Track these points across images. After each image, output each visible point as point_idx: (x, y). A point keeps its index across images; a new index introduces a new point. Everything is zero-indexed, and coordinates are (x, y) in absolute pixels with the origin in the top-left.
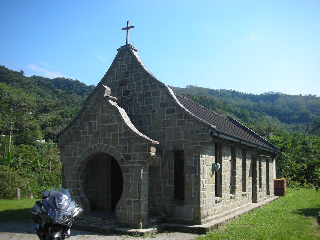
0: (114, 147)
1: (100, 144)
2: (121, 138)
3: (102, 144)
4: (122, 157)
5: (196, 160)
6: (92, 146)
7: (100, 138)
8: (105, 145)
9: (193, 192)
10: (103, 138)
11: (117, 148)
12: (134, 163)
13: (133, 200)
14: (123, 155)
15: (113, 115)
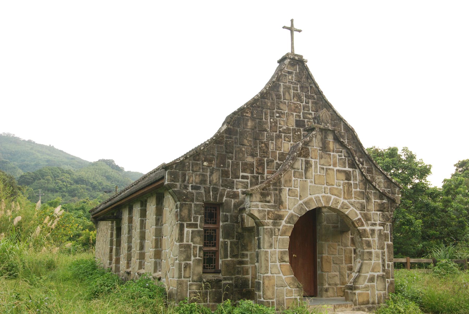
0: (346, 201)
1: (326, 195)
2: (356, 190)
3: (329, 195)
4: (360, 216)
6: (313, 197)
7: (325, 186)
8: (333, 197)
10: (329, 187)
14: (361, 214)
15: (343, 157)
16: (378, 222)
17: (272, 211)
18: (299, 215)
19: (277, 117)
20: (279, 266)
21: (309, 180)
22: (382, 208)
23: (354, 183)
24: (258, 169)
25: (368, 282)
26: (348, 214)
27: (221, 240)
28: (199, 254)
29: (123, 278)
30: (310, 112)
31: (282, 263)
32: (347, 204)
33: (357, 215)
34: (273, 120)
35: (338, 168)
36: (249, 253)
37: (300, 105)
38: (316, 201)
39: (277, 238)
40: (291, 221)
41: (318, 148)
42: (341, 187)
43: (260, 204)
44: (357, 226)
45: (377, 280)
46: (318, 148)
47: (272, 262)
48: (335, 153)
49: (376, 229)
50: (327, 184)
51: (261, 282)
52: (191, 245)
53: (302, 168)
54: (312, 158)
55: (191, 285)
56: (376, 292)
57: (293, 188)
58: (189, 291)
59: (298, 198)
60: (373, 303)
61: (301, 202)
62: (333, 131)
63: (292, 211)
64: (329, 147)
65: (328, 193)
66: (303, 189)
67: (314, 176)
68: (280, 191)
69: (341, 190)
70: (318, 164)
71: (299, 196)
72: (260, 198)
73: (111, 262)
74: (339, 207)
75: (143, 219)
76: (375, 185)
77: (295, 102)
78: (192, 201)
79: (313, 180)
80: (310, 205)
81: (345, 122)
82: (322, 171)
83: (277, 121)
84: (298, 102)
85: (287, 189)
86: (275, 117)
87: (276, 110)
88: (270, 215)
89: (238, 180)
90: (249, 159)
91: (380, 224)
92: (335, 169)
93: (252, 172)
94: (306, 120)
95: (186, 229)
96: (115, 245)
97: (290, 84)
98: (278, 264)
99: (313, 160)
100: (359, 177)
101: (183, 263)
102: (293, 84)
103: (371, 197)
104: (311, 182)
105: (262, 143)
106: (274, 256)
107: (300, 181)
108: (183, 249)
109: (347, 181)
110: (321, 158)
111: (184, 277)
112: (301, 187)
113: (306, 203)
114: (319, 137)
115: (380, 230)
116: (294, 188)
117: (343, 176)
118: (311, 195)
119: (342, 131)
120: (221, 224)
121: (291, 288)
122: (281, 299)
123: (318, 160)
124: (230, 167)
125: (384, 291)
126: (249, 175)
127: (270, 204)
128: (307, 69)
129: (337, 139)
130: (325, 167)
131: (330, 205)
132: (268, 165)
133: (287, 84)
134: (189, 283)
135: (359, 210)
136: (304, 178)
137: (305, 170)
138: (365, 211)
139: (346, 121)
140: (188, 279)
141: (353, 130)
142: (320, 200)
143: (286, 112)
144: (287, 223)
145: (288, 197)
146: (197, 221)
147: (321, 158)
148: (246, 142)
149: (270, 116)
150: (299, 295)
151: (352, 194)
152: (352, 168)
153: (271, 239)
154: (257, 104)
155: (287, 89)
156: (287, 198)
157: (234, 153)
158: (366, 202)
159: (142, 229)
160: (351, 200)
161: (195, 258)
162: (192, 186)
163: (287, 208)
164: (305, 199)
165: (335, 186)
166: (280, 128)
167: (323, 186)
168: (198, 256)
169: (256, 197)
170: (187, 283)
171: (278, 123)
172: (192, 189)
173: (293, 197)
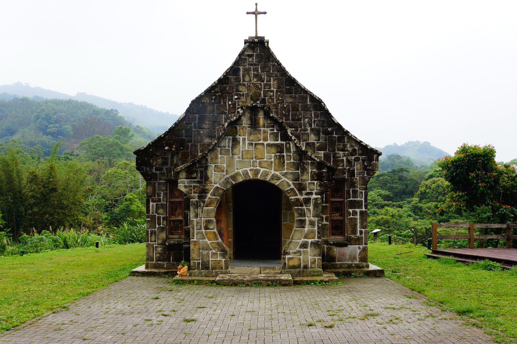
0: (278, 173)
2: (289, 161)
3: (258, 168)
4: (292, 186)
5: (362, 193)
7: (254, 159)
8: (262, 170)
9: (359, 229)
10: (258, 161)
11: (285, 175)
12: (311, 194)
13: (310, 241)
14: (293, 184)
15: (275, 131)
16: (314, 192)
17: (197, 186)
18: (224, 188)
19: (235, 99)
20: (204, 233)
21: (236, 156)
22: (318, 177)
23: (287, 155)
25: (300, 247)
26: (278, 185)
28: (163, 223)
30: (272, 89)
31: (207, 231)
32: (278, 175)
33: (289, 185)
34: (232, 102)
35: (269, 142)
37: (261, 85)
38: (243, 174)
39: (203, 209)
40: (216, 194)
41: (247, 126)
42: (273, 160)
43: (186, 180)
45: (311, 246)
46: (247, 126)
47: (197, 230)
48: (266, 128)
49: (311, 198)
50: (256, 158)
52: (156, 216)
53: (228, 145)
54: (240, 135)
55: (156, 247)
56: (310, 257)
58: (155, 252)
59: (225, 173)
60: (306, 267)
61: (228, 176)
62: (262, 108)
63: (218, 185)
64: (259, 123)
65: (257, 167)
66: (230, 165)
67: (242, 151)
68: (206, 168)
69: (272, 163)
70: (246, 140)
71: (225, 171)
72: (187, 176)
74: (268, 179)
76: (310, 155)
77: (256, 82)
78: (156, 179)
80: (236, 178)
81: (311, 94)
82: (251, 147)
83: (236, 103)
84: (259, 82)
85: (214, 165)
86: (234, 100)
87: (234, 93)
88: (196, 189)
91: (317, 193)
92: (265, 143)
94: (267, 98)
95: (151, 203)
97: (250, 67)
98: (203, 230)
99: (241, 137)
100: (293, 149)
101: (150, 230)
102: (253, 65)
103: (306, 167)
104: (239, 158)
105: (220, 125)
106: (199, 224)
107: (227, 157)
108: (149, 219)
109: (279, 154)
110: (250, 134)
111: (151, 241)
112: (227, 163)
113: (234, 177)
114: (247, 115)
115: (316, 199)
116: (220, 165)
117: (274, 150)
118: (237, 169)
119: (309, 103)
122: (205, 260)
123: (246, 137)
124: (189, 149)
125: (319, 256)
127: (196, 180)
128: (268, 49)
129: (267, 115)
130: (254, 143)
131: (258, 178)
133: (247, 67)
134: (155, 246)
135: (292, 181)
136: (231, 154)
137: (232, 148)
138: (299, 181)
139: (312, 93)
140: (154, 243)
141: (320, 100)
142: (248, 173)
143: (245, 93)
144: (212, 196)
145: (213, 172)
146: (160, 196)
147: (250, 134)
148: (204, 126)
150: (223, 258)
151: (284, 166)
152: (286, 141)
153: (197, 210)
155: (247, 71)
156: (213, 174)
157: (193, 136)
158: (301, 172)
160: (282, 171)
163: (213, 183)
164: (233, 173)
165: (265, 159)
167: (252, 161)
168: (162, 224)
169: (182, 175)
170: (153, 245)
171: (237, 104)
173: (219, 173)
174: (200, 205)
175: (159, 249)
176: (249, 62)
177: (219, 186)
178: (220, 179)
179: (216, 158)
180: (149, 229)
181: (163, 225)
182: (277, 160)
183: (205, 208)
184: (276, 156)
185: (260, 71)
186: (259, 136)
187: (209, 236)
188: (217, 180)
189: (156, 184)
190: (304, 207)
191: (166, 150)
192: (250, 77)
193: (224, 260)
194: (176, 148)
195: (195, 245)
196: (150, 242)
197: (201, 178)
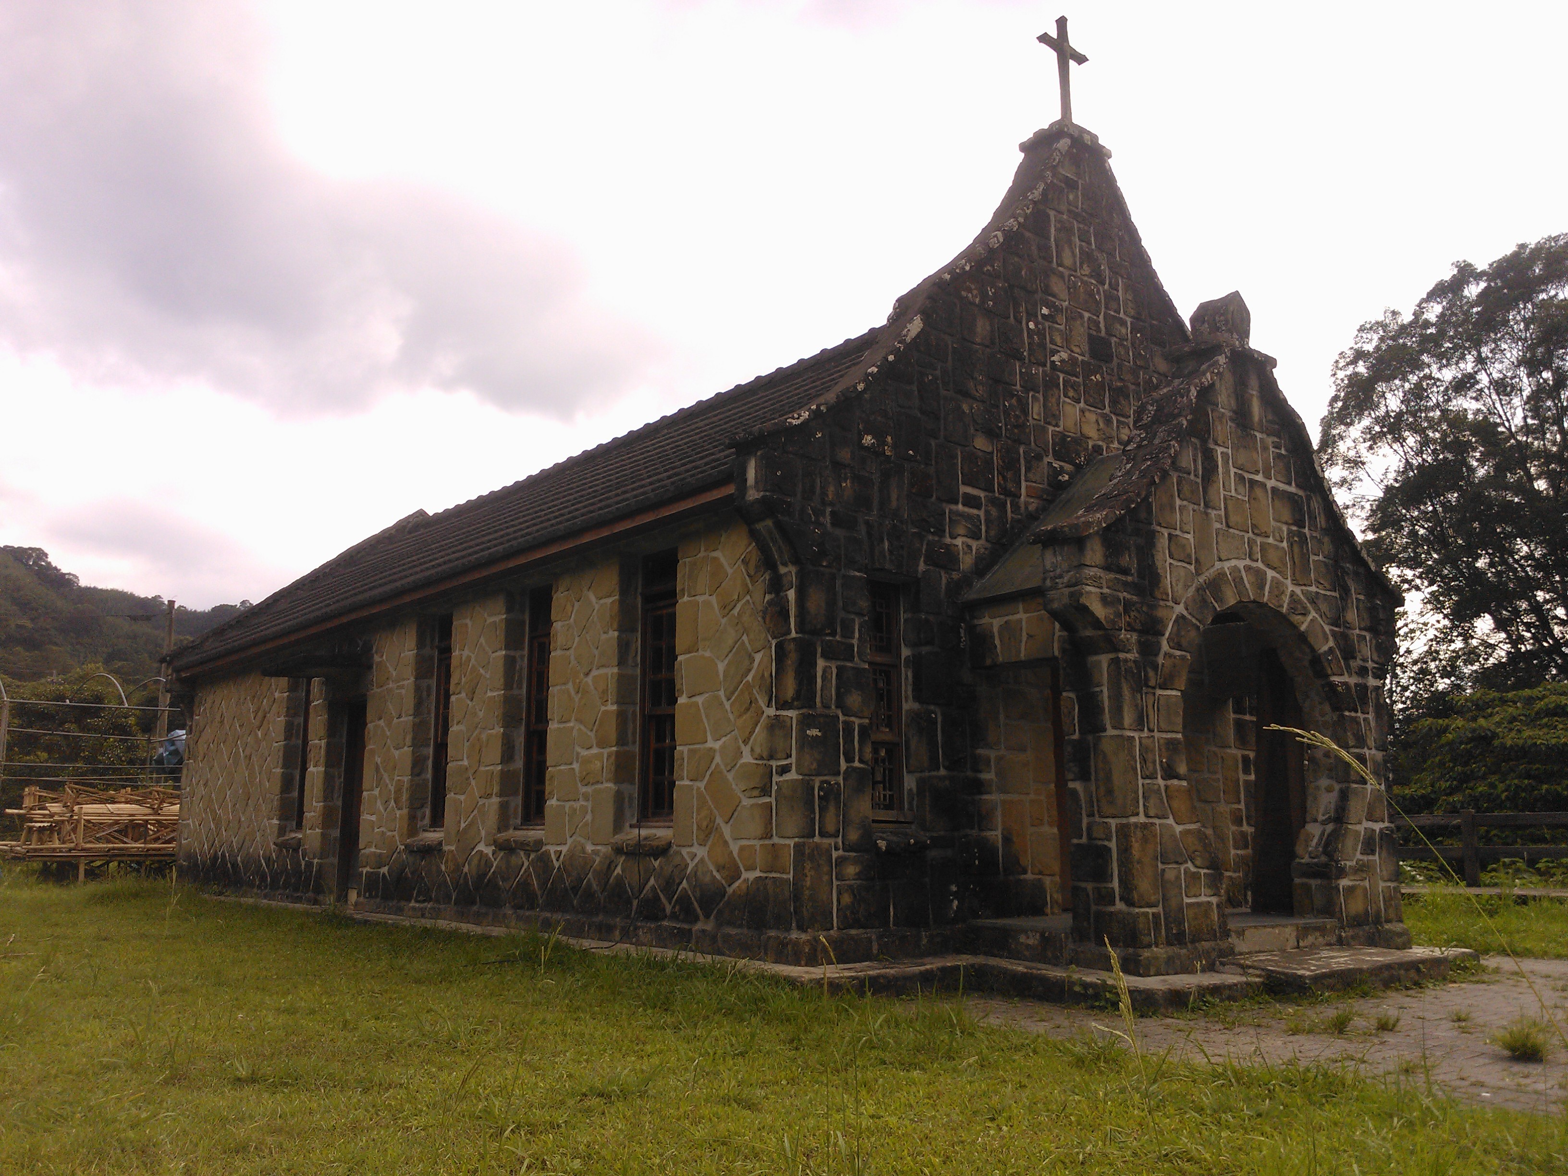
0: (1298, 590)
1: (1254, 565)
3: (1260, 565)
6: (1227, 565)
10: (1259, 540)
14: (1334, 634)
15: (1283, 452)
19: (1043, 316)
20: (1163, 789)
21: (1213, 513)
24: (1004, 478)
26: (1307, 631)
27: (908, 705)
28: (860, 750)
29: (385, 870)
30: (1122, 315)
31: (1169, 782)
36: (992, 754)
37: (1098, 292)
38: (1234, 580)
44: (1329, 672)
45: (1381, 847)
50: (1256, 531)
51: (1113, 845)
53: (1195, 471)
54: (1217, 444)
55: (841, 861)
57: (1178, 532)
58: (835, 883)
73: (286, 826)
75: (512, 653)
79: (1222, 513)
83: (1044, 329)
85: (1166, 533)
89: (953, 507)
90: (981, 443)
93: (989, 489)
94: (1114, 340)
95: (821, 663)
96: (322, 760)
99: (1220, 450)
105: (1012, 396)
108: (814, 732)
111: (822, 834)
120: (905, 652)
121: (1196, 867)
126: (982, 494)
127: (1130, 579)
130: (1247, 476)
132: (1028, 470)
140: (832, 841)
149: (1027, 313)
153: (1139, 696)
154: (993, 267)
159: (512, 688)
161: (849, 765)
162: (832, 513)
166: (1054, 353)
167: (1246, 536)
172: (833, 524)
174: (1147, 678)
175: (851, 870)
176: (1069, 203)
177: (1185, 613)
178: (1186, 587)
179: (1172, 508)
180: (818, 775)
181: (861, 761)
182: (1296, 549)
183: (1159, 692)
184: (1290, 532)
185: (1093, 247)
186: (1255, 455)
187: (1175, 804)
188: (1179, 588)
189: (838, 583)
190: (1359, 714)
191: (867, 449)
192: (1074, 255)
193: (1214, 900)
194: (895, 446)
195: (1145, 840)
196: (817, 839)
197: (1141, 574)
